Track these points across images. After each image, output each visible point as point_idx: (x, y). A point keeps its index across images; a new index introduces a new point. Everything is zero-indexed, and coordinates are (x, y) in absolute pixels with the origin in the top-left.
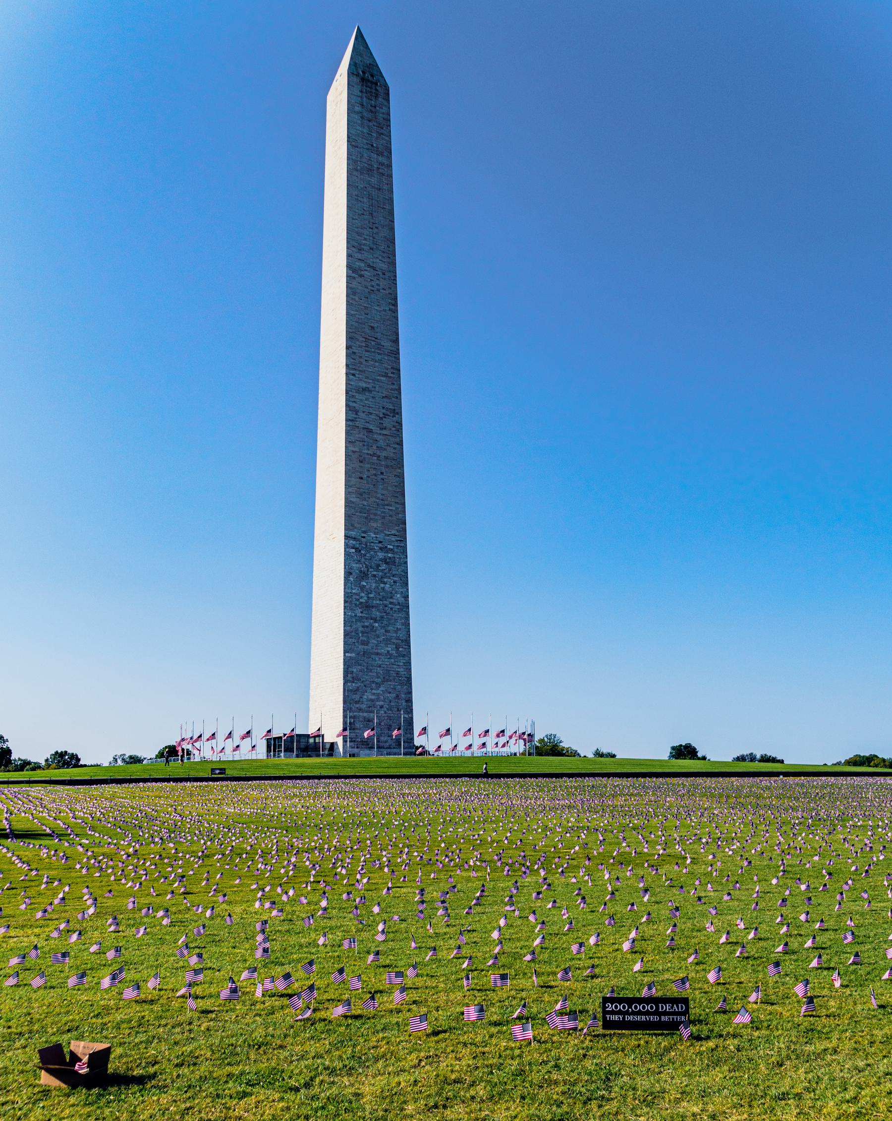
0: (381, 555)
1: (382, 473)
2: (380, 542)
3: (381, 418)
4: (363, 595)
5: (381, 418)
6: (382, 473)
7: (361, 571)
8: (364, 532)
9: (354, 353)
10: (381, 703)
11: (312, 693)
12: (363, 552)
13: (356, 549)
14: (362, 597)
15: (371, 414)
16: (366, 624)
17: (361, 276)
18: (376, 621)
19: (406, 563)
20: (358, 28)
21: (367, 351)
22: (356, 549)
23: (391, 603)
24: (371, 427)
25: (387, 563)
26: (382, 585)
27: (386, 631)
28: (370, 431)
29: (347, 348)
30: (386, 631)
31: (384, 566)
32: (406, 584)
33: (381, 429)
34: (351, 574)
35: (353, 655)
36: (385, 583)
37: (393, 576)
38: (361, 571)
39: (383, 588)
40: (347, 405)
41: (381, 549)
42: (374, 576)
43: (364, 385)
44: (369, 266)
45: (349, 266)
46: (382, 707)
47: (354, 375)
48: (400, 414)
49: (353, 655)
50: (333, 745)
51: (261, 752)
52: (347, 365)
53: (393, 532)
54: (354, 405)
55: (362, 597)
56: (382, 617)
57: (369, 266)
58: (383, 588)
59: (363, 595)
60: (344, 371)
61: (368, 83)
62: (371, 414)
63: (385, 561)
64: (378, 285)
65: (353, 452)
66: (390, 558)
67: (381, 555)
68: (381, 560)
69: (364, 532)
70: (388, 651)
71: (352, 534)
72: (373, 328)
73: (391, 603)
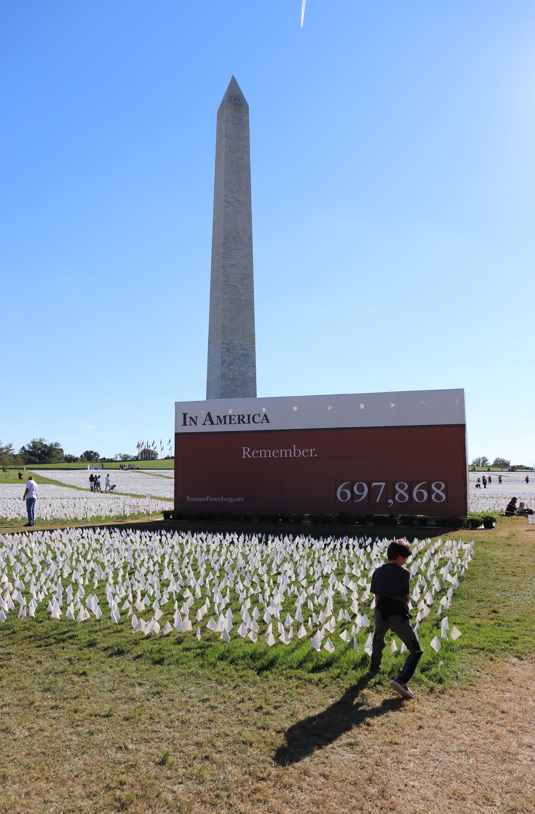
0: (241, 352)
1: (242, 309)
3: (242, 280)
5: (242, 280)
6: (242, 309)
7: (230, 361)
8: (232, 340)
12: (231, 351)
13: (228, 349)
14: (230, 375)
15: (236, 277)
16: (233, 389)
17: (233, 206)
18: (238, 387)
19: (255, 356)
21: (235, 245)
22: (228, 349)
23: (246, 377)
24: (236, 285)
25: (244, 356)
27: (244, 392)
28: (236, 287)
30: (244, 392)
31: (242, 358)
32: (255, 367)
33: (242, 285)
34: (225, 362)
36: (243, 367)
37: (248, 363)
38: (230, 361)
39: (242, 370)
41: (241, 349)
42: (237, 363)
43: (233, 263)
44: (236, 200)
47: (227, 258)
48: (252, 277)
53: (248, 340)
54: (227, 273)
55: (230, 375)
56: (241, 385)
57: (236, 200)
58: (242, 370)
62: (236, 277)
63: (243, 355)
64: (241, 209)
67: (241, 352)
68: (241, 355)
69: (232, 340)
72: (238, 232)
73: (246, 377)
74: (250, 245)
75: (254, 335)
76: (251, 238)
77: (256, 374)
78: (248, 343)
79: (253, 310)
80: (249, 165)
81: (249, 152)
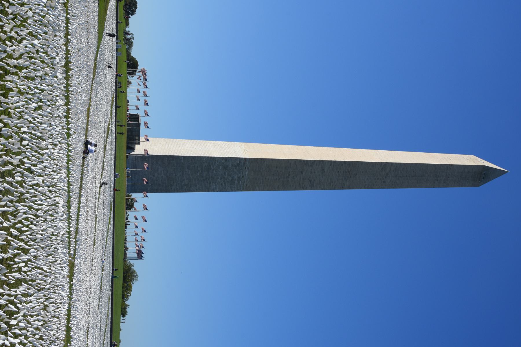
0: (236, 177)
2: (243, 177)
4: (215, 167)
6: (280, 179)
9: (342, 165)
10: (156, 176)
11: (162, 139)
12: (237, 168)
16: (199, 168)
19: (232, 191)
20: (504, 172)
21: (343, 172)
22: (239, 164)
23: (210, 182)
26: (220, 178)
29: (345, 162)
31: (230, 178)
32: (221, 191)
35: (182, 161)
37: (225, 184)
40: (315, 161)
41: (239, 177)
42: (225, 173)
45: (387, 163)
46: (154, 176)
47: (331, 165)
48: (311, 189)
49: (182, 161)
50: (133, 149)
51: (132, 111)
52: (336, 161)
59: (215, 167)
60: (333, 160)
61: (479, 176)
65: (291, 164)
66: (234, 182)
67: (236, 177)
69: (248, 168)
70: (184, 180)
71: (247, 162)
72: (356, 175)
73: (210, 182)
74: (342, 187)
75: (254, 190)
76: (349, 188)
77: (214, 191)
78: (245, 184)
79: (278, 189)
80: (421, 187)
81: (434, 187)
